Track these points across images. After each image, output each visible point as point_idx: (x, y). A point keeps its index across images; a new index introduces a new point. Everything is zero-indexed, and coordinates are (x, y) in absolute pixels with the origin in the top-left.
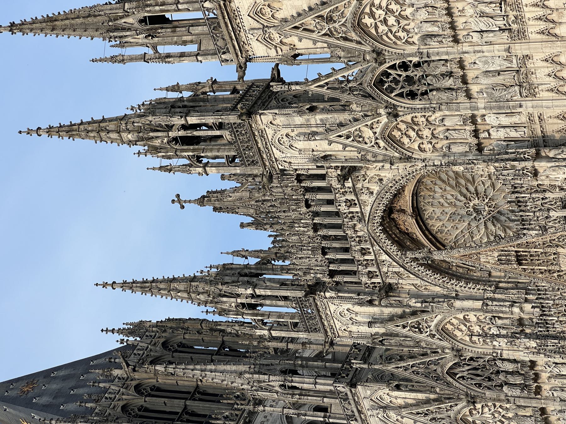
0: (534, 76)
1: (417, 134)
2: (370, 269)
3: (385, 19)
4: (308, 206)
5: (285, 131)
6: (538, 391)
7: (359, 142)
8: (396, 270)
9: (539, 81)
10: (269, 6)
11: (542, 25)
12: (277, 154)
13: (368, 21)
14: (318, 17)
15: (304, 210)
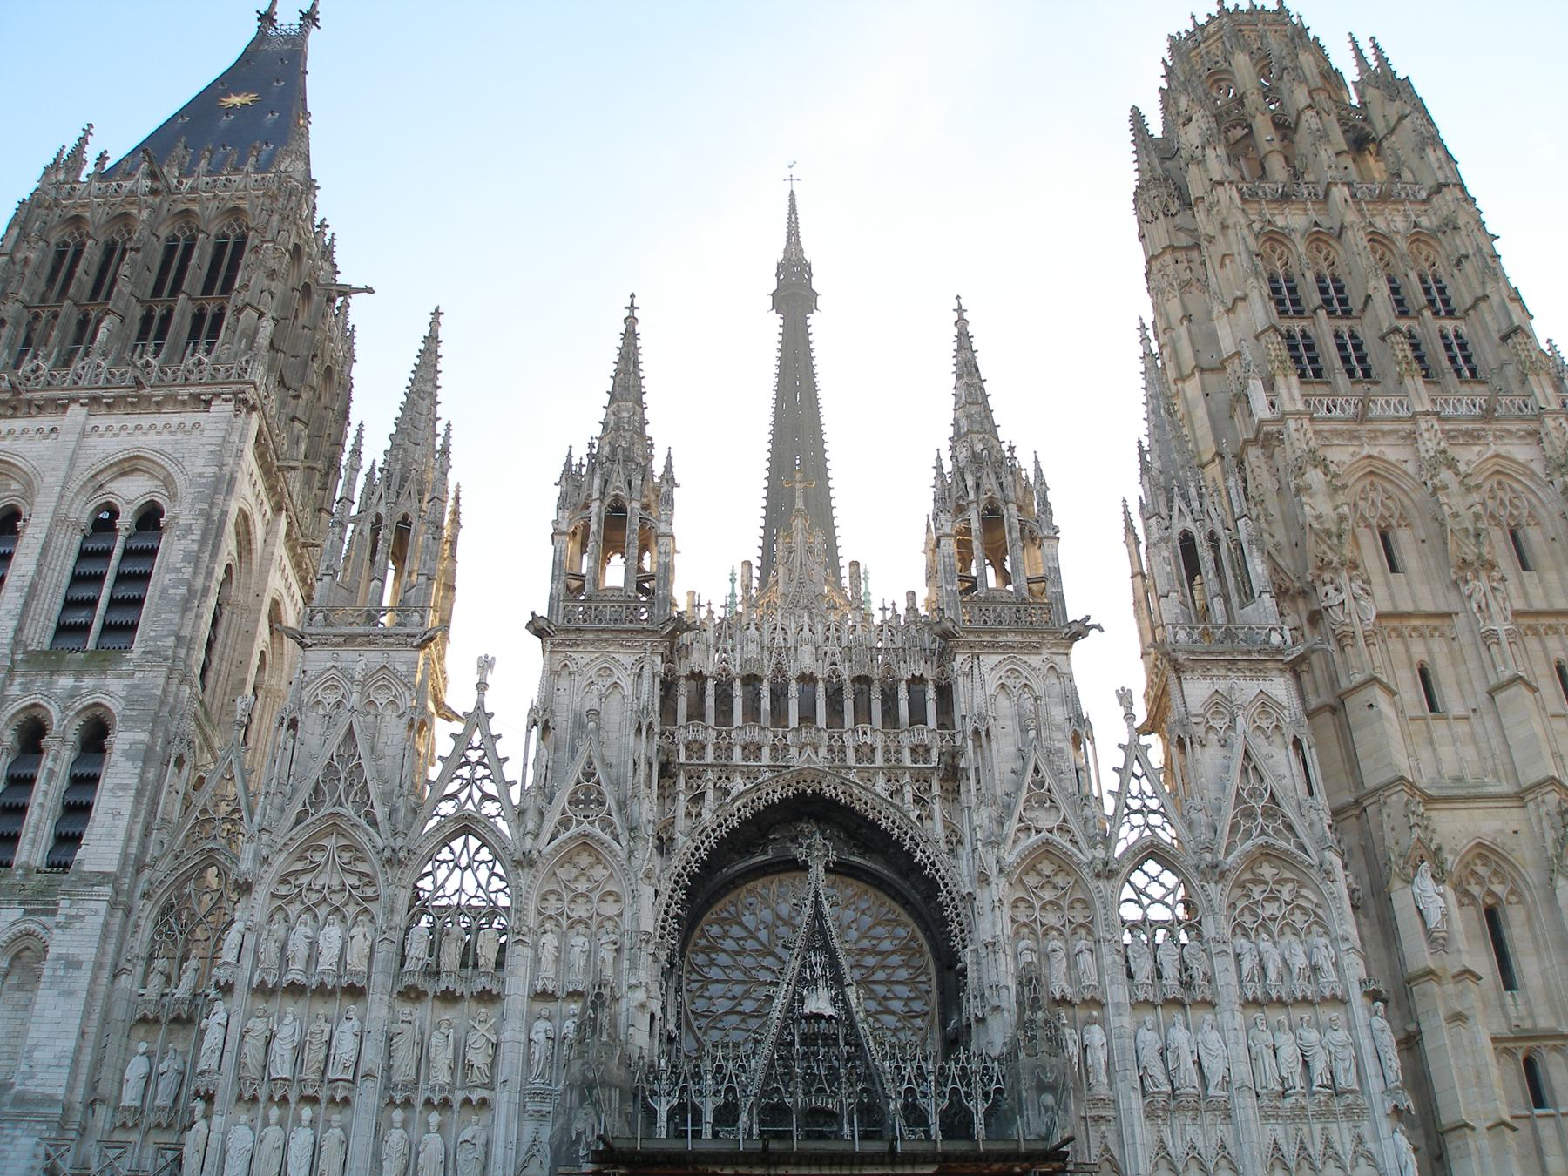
0: (1189, 1121)
1: (1051, 902)
2: (710, 750)
3: (1277, 899)
4: (858, 680)
5: (1038, 689)
6: (412, 994)
7: (1027, 801)
8: (710, 795)
9: (1178, 1130)
10: (1277, 727)
11: (1290, 1151)
12: (989, 660)
13: (1267, 871)
14: (1272, 795)
15: (846, 675)
